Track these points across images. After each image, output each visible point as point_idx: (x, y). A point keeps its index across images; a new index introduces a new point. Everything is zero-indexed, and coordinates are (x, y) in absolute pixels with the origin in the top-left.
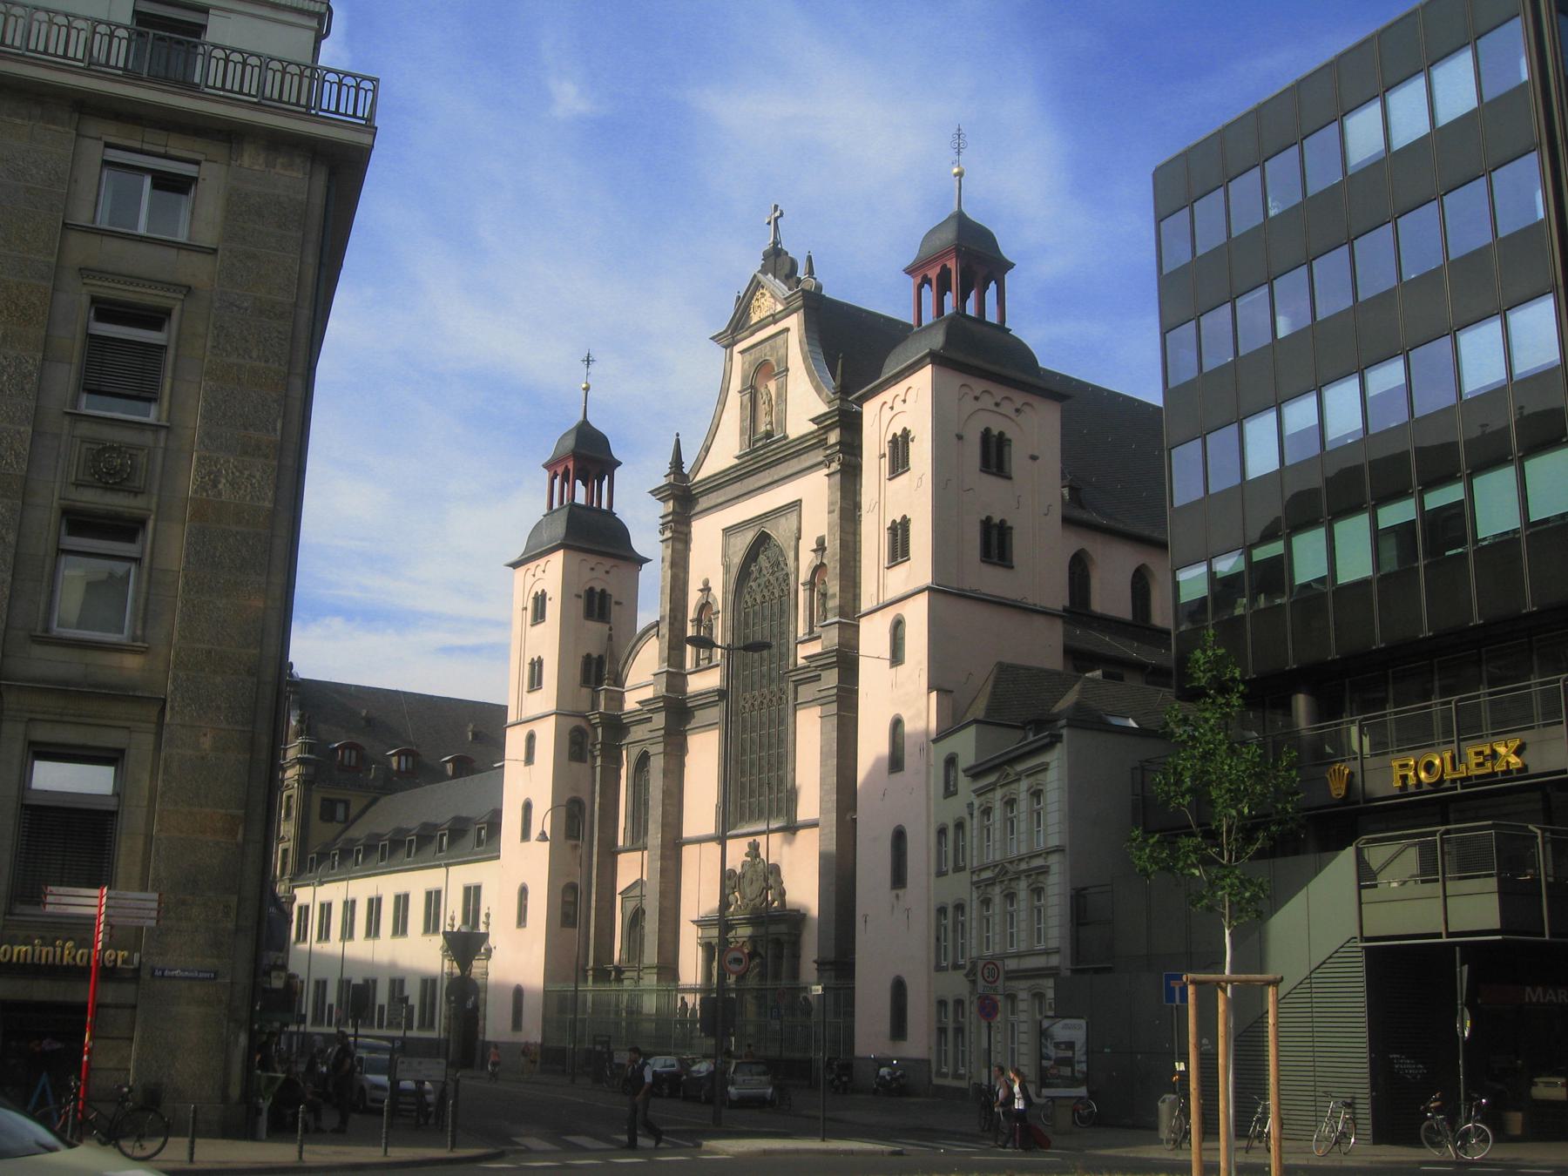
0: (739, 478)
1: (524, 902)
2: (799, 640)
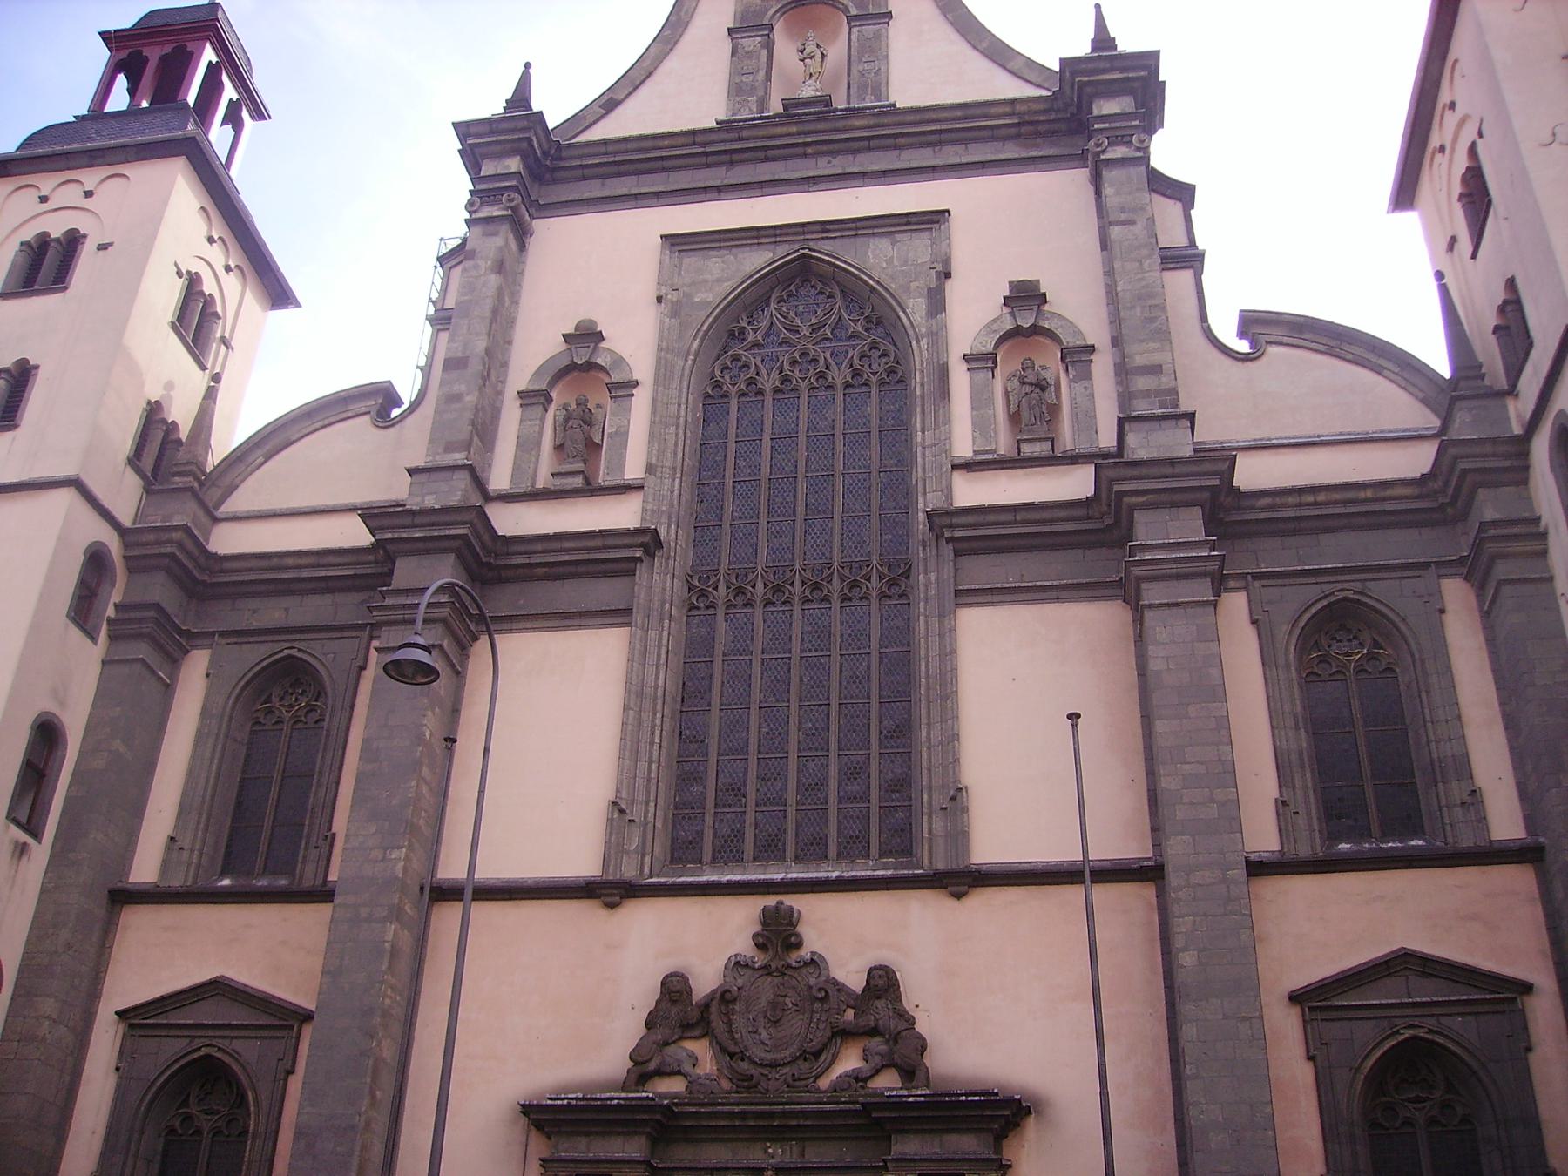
0: (730, 158)
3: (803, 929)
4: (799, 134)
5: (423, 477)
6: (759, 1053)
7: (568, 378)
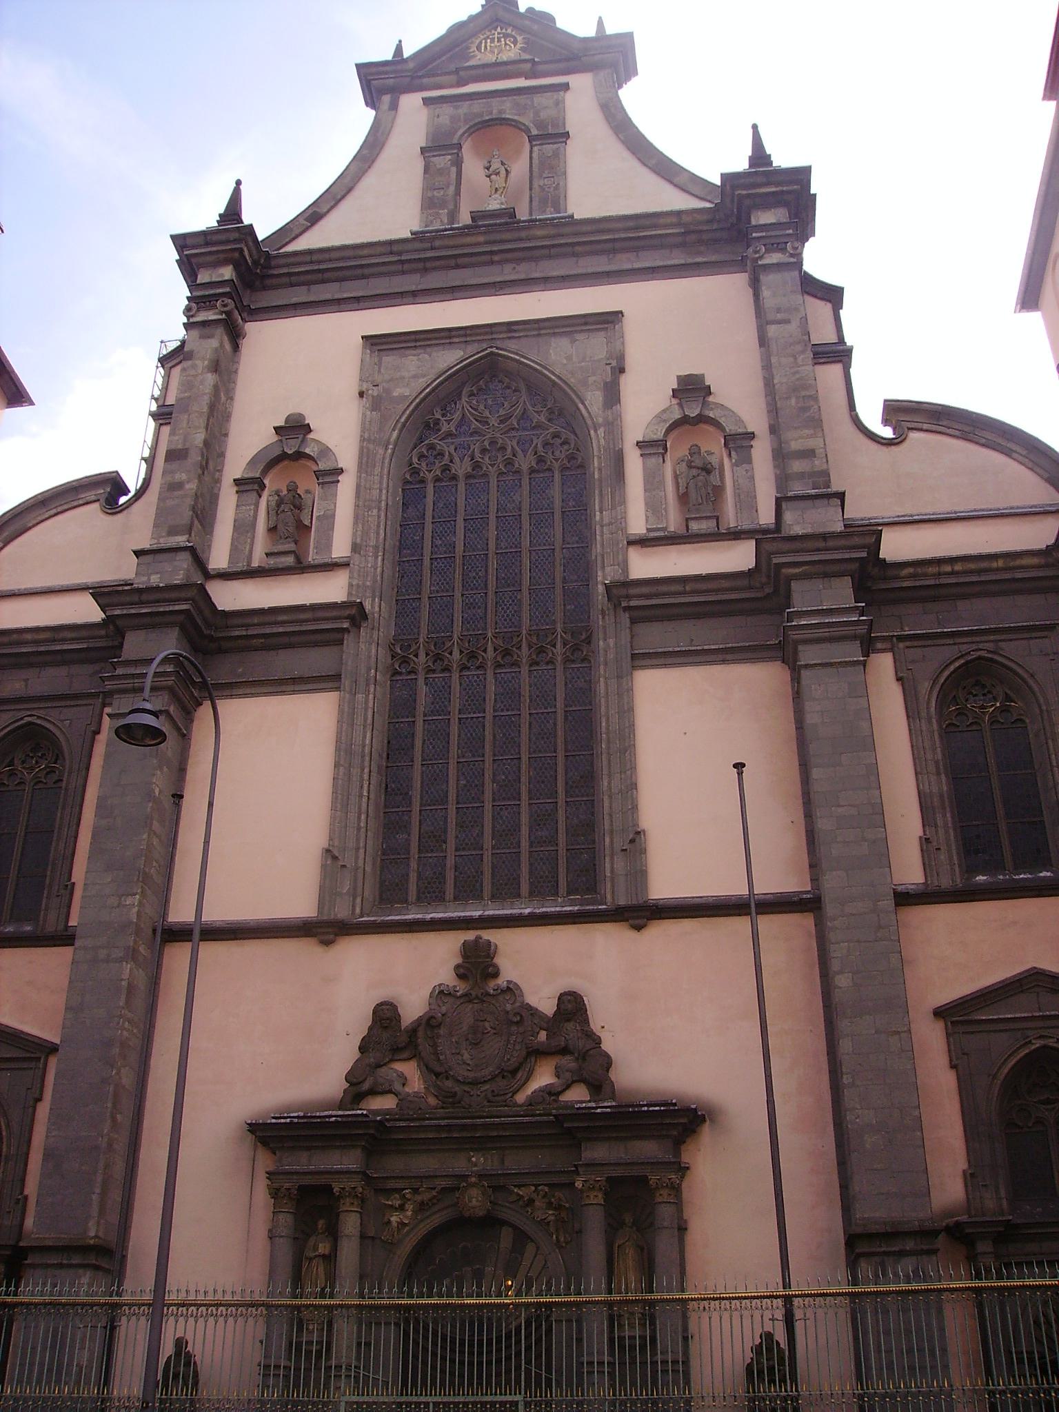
0: (424, 266)
3: (500, 961)
4: (486, 243)
5: (147, 559)
6: (462, 1072)
7: (281, 465)
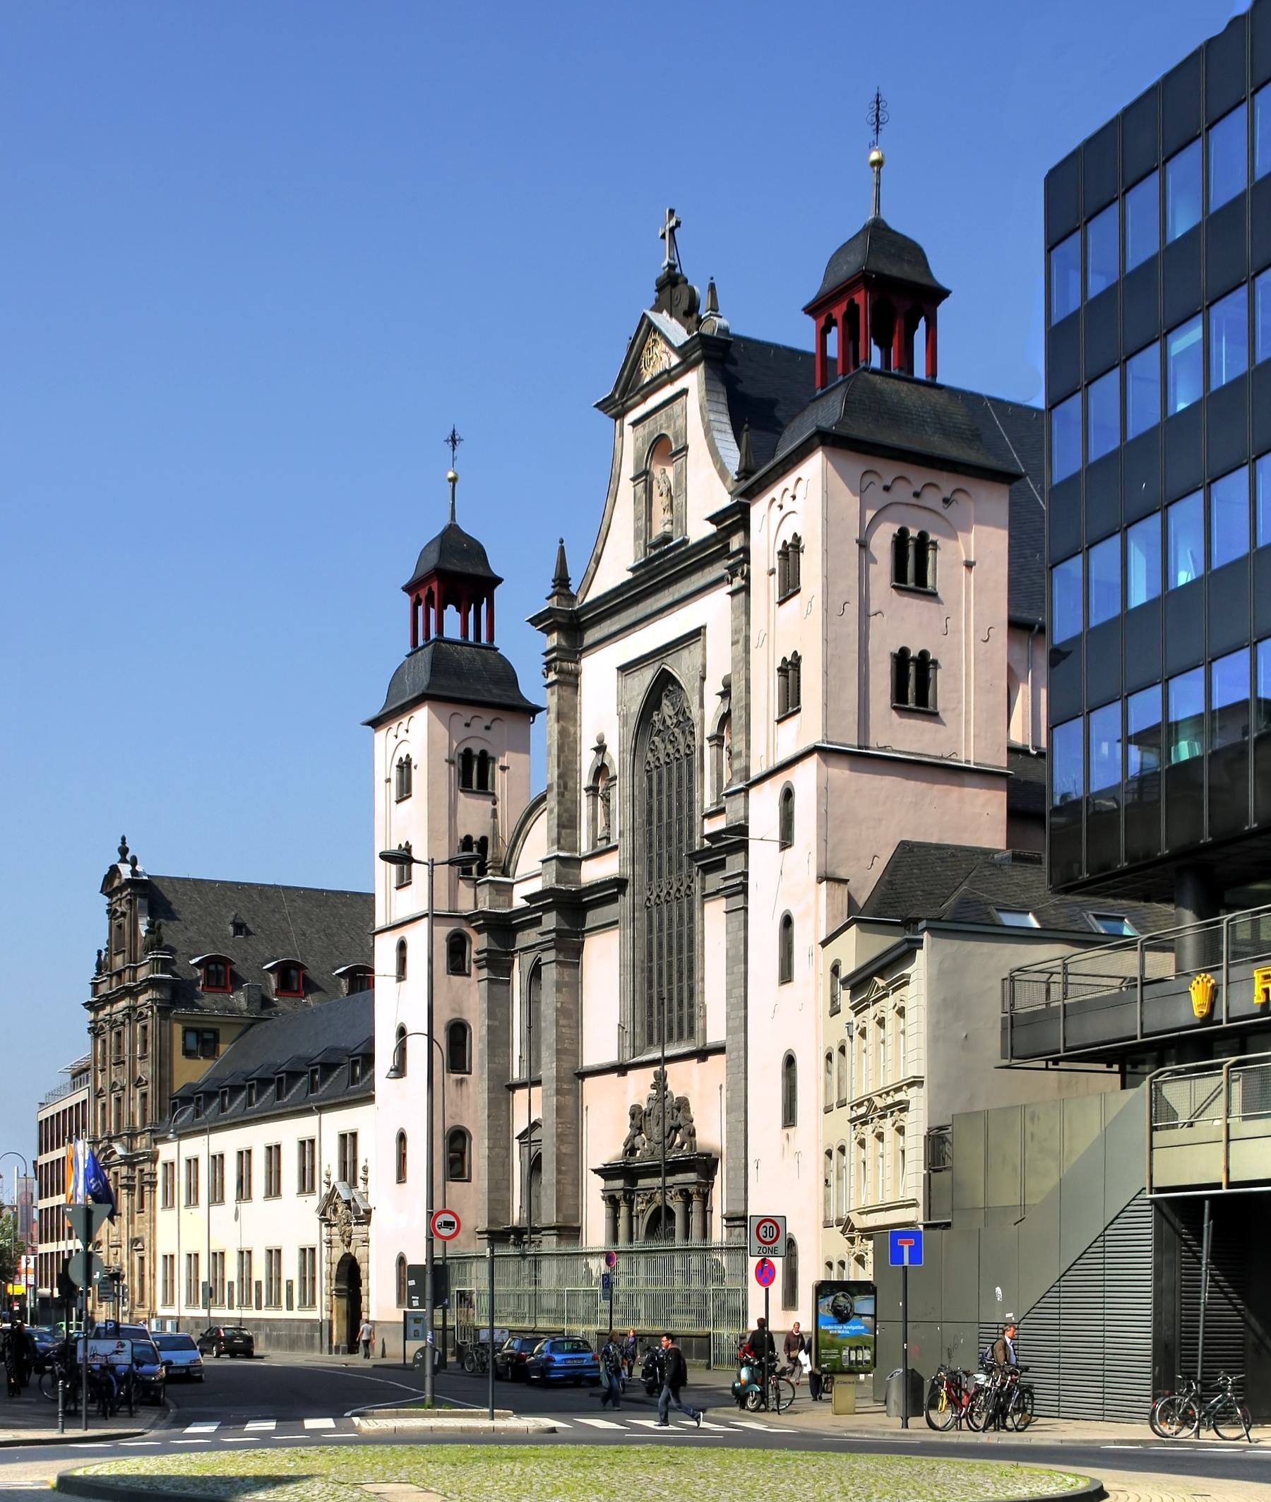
1: (403, 1151)
2: (705, 812)
